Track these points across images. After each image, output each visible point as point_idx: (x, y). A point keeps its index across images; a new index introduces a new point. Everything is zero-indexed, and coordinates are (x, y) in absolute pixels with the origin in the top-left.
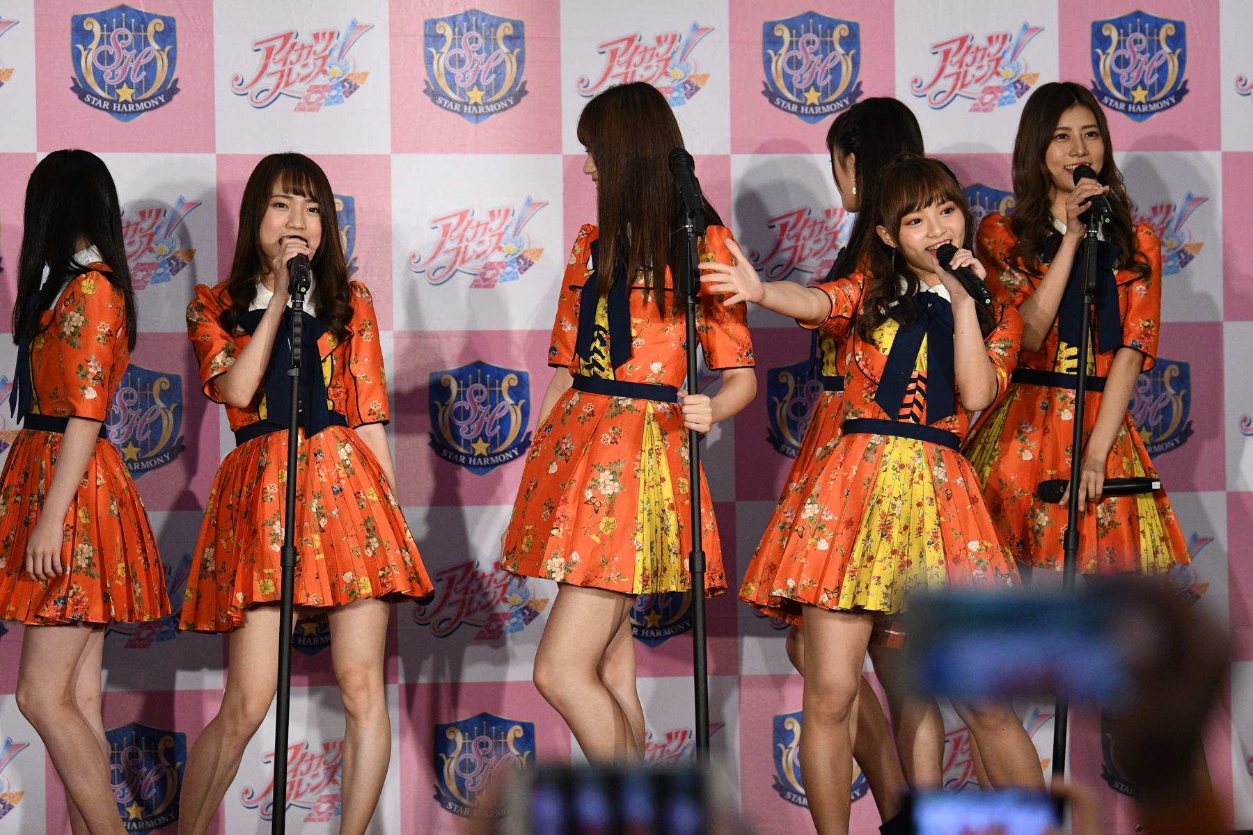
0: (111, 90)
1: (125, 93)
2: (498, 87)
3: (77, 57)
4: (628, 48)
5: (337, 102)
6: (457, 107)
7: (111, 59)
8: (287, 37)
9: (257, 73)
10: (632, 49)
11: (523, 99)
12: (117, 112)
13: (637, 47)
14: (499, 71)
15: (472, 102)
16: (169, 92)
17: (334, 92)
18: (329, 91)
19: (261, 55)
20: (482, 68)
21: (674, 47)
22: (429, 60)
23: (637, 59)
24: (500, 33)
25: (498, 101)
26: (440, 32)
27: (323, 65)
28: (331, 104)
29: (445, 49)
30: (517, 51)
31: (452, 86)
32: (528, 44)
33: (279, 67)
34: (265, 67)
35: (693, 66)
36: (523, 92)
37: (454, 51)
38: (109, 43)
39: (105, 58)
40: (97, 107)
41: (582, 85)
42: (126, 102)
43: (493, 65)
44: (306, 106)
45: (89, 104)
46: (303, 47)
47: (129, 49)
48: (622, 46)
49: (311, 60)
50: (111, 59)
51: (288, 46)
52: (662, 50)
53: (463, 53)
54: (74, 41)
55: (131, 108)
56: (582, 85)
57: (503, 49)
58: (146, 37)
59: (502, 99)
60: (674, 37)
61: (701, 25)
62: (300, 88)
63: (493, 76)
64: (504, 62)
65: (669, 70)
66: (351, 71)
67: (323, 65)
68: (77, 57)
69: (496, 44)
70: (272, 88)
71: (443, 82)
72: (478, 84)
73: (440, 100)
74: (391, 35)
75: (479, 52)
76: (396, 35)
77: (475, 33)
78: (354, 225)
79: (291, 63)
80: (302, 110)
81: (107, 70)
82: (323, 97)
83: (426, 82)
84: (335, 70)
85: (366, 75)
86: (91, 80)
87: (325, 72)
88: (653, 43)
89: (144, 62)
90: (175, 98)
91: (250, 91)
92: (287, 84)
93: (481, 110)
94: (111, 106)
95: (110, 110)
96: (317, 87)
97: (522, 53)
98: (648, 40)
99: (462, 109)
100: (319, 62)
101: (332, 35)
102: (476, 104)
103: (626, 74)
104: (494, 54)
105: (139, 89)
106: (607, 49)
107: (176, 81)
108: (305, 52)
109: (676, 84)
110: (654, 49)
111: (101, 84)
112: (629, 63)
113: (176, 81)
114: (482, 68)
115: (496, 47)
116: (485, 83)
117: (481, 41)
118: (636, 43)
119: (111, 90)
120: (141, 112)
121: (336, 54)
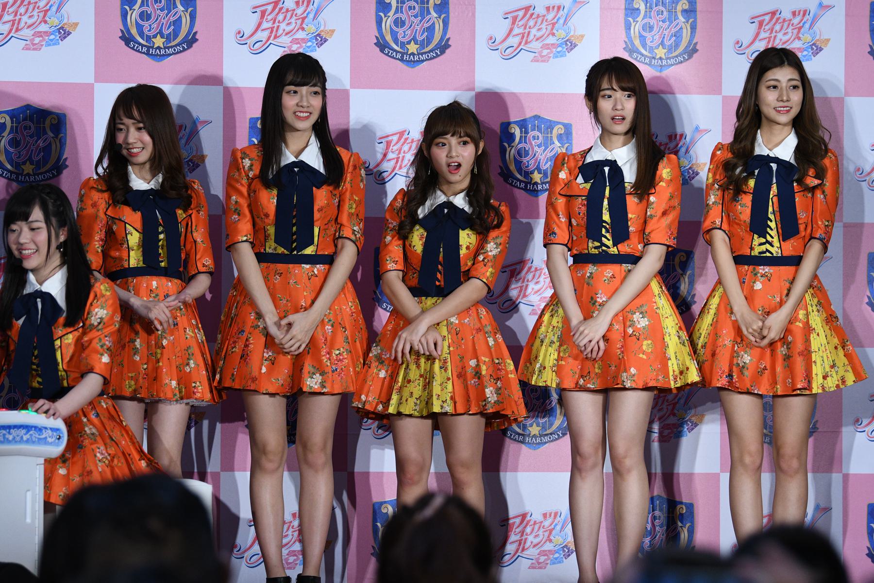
0: (403, 45)
1: (413, 48)
2: (677, 46)
3: (379, 22)
4: (771, 20)
5: (561, 56)
6: (647, 60)
7: (403, 23)
8: (527, 9)
9: (505, 35)
10: (774, 20)
11: (695, 55)
12: (406, 61)
13: (778, 19)
14: (678, 35)
15: (658, 57)
16: (443, 47)
17: (559, 49)
18: (556, 48)
19: (508, 22)
20: (666, 32)
21: (805, 19)
22: (628, 27)
23: (778, 27)
24: (679, 8)
25: (677, 56)
26: (636, 7)
27: (552, 29)
28: (557, 57)
29: (639, 19)
30: (691, 20)
31: (644, 45)
32: (699, 16)
33: (521, 30)
34: (511, 30)
35: (818, 33)
36: (695, 50)
37: (646, 21)
38: (402, 12)
39: (399, 23)
40: (393, 57)
41: (737, 46)
42: (413, 54)
43: (674, 30)
44: (540, 58)
45: (387, 55)
46: (538, 16)
47: (416, 16)
48: (767, 18)
49: (543, 26)
50: (403, 23)
51: (528, 16)
52: (796, 21)
53: (652, 22)
54: (378, 11)
55: (416, 58)
56: (737, 46)
57: (681, 19)
58: (428, 8)
59: (680, 55)
60: (805, 12)
61: (825, 3)
62: (536, 45)
63: (674, 38)
64: (681, 28)
65: (800, 35)
66: (572, 34)
67: (552, 29)
68: (379, 22)
69: (676, 15)
70: (515, 46)
71: (637, 42)
72: (662, 43)
73: (635, 55)
74: (601, 8)
75: (663, 21)
76: (604, 8)
77: (661, 8)
78: (571, 144)
79: (530, 28)
80: (538, 61)
81: (400, 31)
82: (552, 52)
83: (626, 42)
84: (561, 33)
85: (582, 36)
86: (389, 38)
87: (553, 34)
88: (788, 16)
89: (426, 25)
90: (447, 51)
91: (500, 47)
92: (526, 43)
93: (664, 63)
94: (402, 56)
95: (402, 60)
96: (547, 44)
97: (695, 22)
98: (786, 14)
99: (651, 62)
100: (549, 27)
101: (559, 8)
102: (661, 58)
103: (770, 38)
104: (675, 23)
105: (422, 45)
106: (756, 20)
107: (449, 39)
108: (540, 20)
109: (806, 45)
110: (790, 20)
111: (396, 41)
112: (772, 30)
113: (449, 39)
114: (666, 32)
115: (676, 18)
116: (667, 43)
117: (665, 13)
118: (777, 16)
119: (403, 45)
120: (423, 61)
121: (561, 21)
